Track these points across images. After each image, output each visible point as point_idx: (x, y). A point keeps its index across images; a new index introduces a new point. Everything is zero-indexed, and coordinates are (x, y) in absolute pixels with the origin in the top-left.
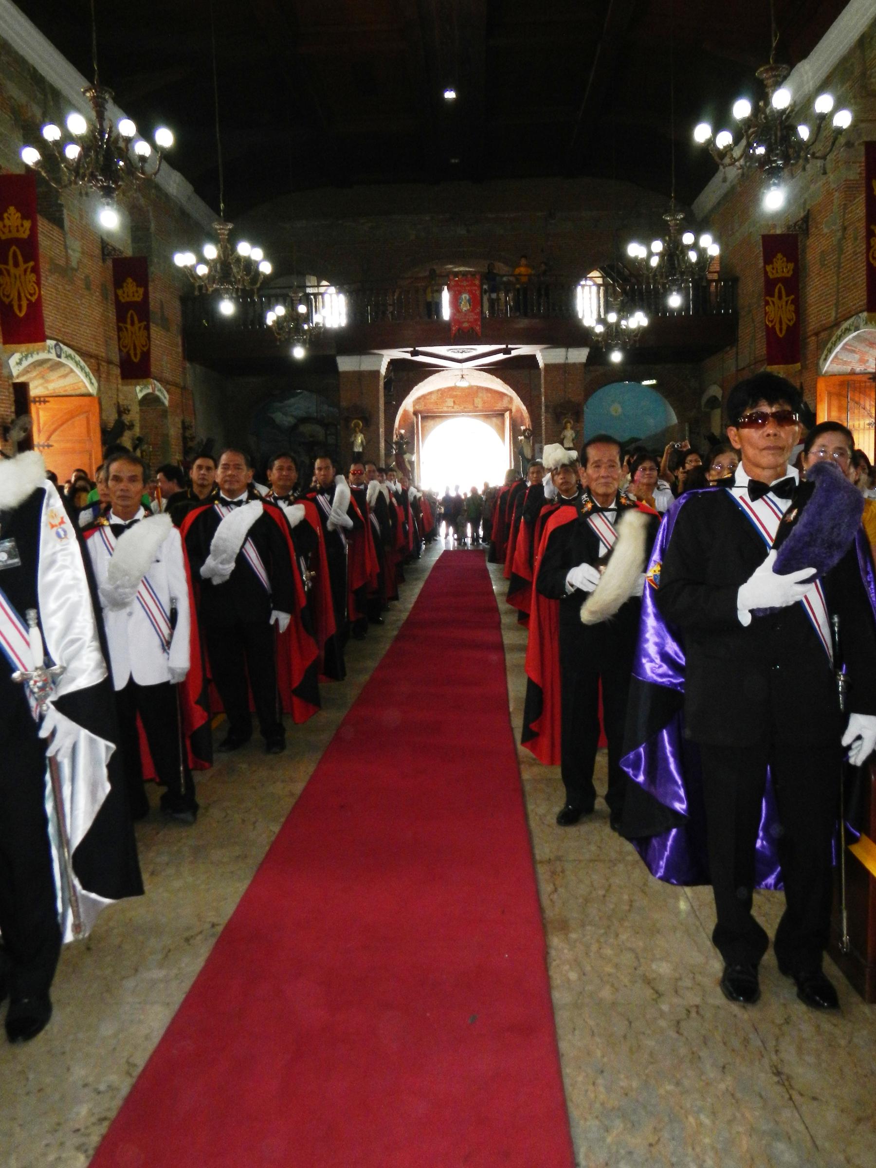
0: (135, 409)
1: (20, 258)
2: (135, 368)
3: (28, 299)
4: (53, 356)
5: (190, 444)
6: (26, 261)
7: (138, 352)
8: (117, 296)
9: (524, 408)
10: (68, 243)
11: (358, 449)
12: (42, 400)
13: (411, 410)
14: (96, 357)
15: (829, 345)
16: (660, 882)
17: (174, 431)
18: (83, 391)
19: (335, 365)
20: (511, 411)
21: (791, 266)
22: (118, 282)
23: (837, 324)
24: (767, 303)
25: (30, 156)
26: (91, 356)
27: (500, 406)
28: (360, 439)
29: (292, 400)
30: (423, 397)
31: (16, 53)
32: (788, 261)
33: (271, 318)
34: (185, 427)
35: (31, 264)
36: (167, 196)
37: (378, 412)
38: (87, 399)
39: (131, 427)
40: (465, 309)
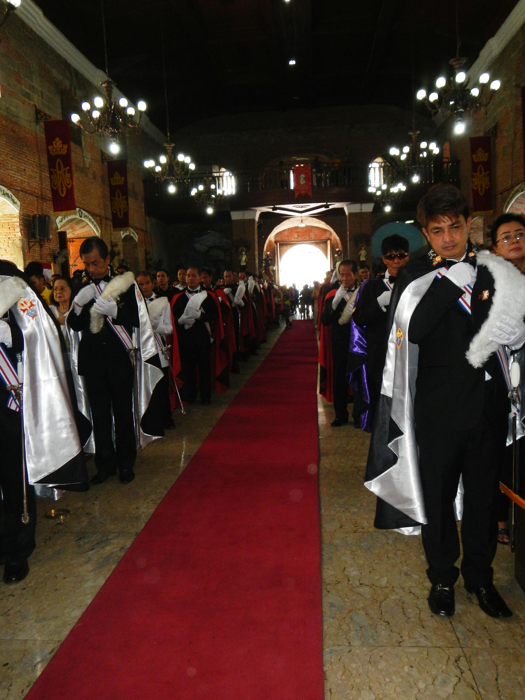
0: (120, 244)
2: (120, 221)
3: (66, 187)
4: (78, 216)
6: (65, 167)
7: (122, 212)
8: (110, 182)
9: (338, 238)
10: (84, 154)
11: (243, 264)
12: (72, 240)
13: (273, 240)
14: (100, 216)
15: (508, 200)
16: (364, 432)
17: (141, 256)
19: (230, 217)
20: (331, 240)
21: (487, 154)
22: (111, 175)
23: (512, 188)
24: (473, 176)
26: (97, 216)
29: (205, 237)
31: (56, 52)
32: (485, 152)
33: (194, 192)
34: (147, 253)
35: (68, 168)
37: (254, 243)
39: (119, 254)
40: (302, 183)
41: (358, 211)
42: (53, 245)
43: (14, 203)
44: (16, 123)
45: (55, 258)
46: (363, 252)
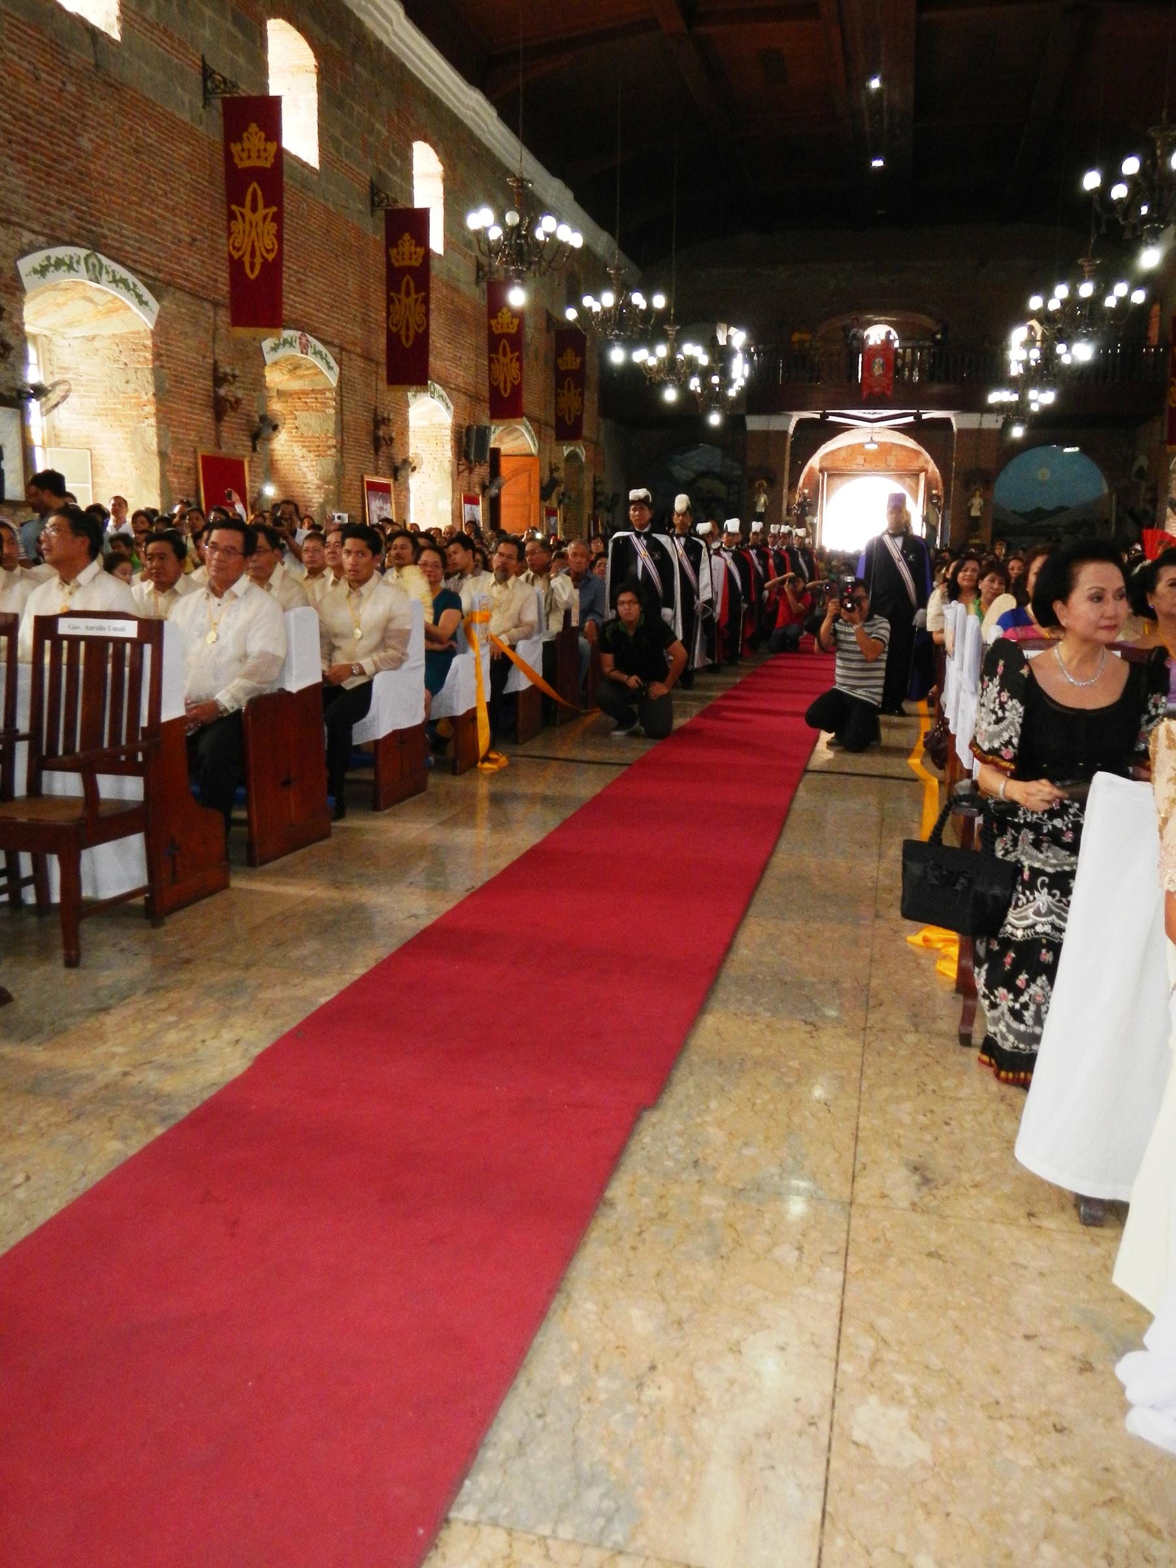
0: (562, 466)
1: (508, 349)
5: (601, 499)
6: (512, 352)
7: (573, 415)
11: (760, 509)
17: (588, 487)
18: (527, 451)
19: (744, 425)
20: (926, 471)
22: (559, 353)
25: (571, 314)
27: (915, 465)
28: (763, 499)
29: (693, 453)
30: (832, 453)
34: (596, 483)
35: (517, 354)
36: (595, 256)
38: (530, 459)
41: (975, 426)
42: (483, 471)
43: (448, 408)
44: (455, 290)
45: (484, 488)
46: (977, 502)
